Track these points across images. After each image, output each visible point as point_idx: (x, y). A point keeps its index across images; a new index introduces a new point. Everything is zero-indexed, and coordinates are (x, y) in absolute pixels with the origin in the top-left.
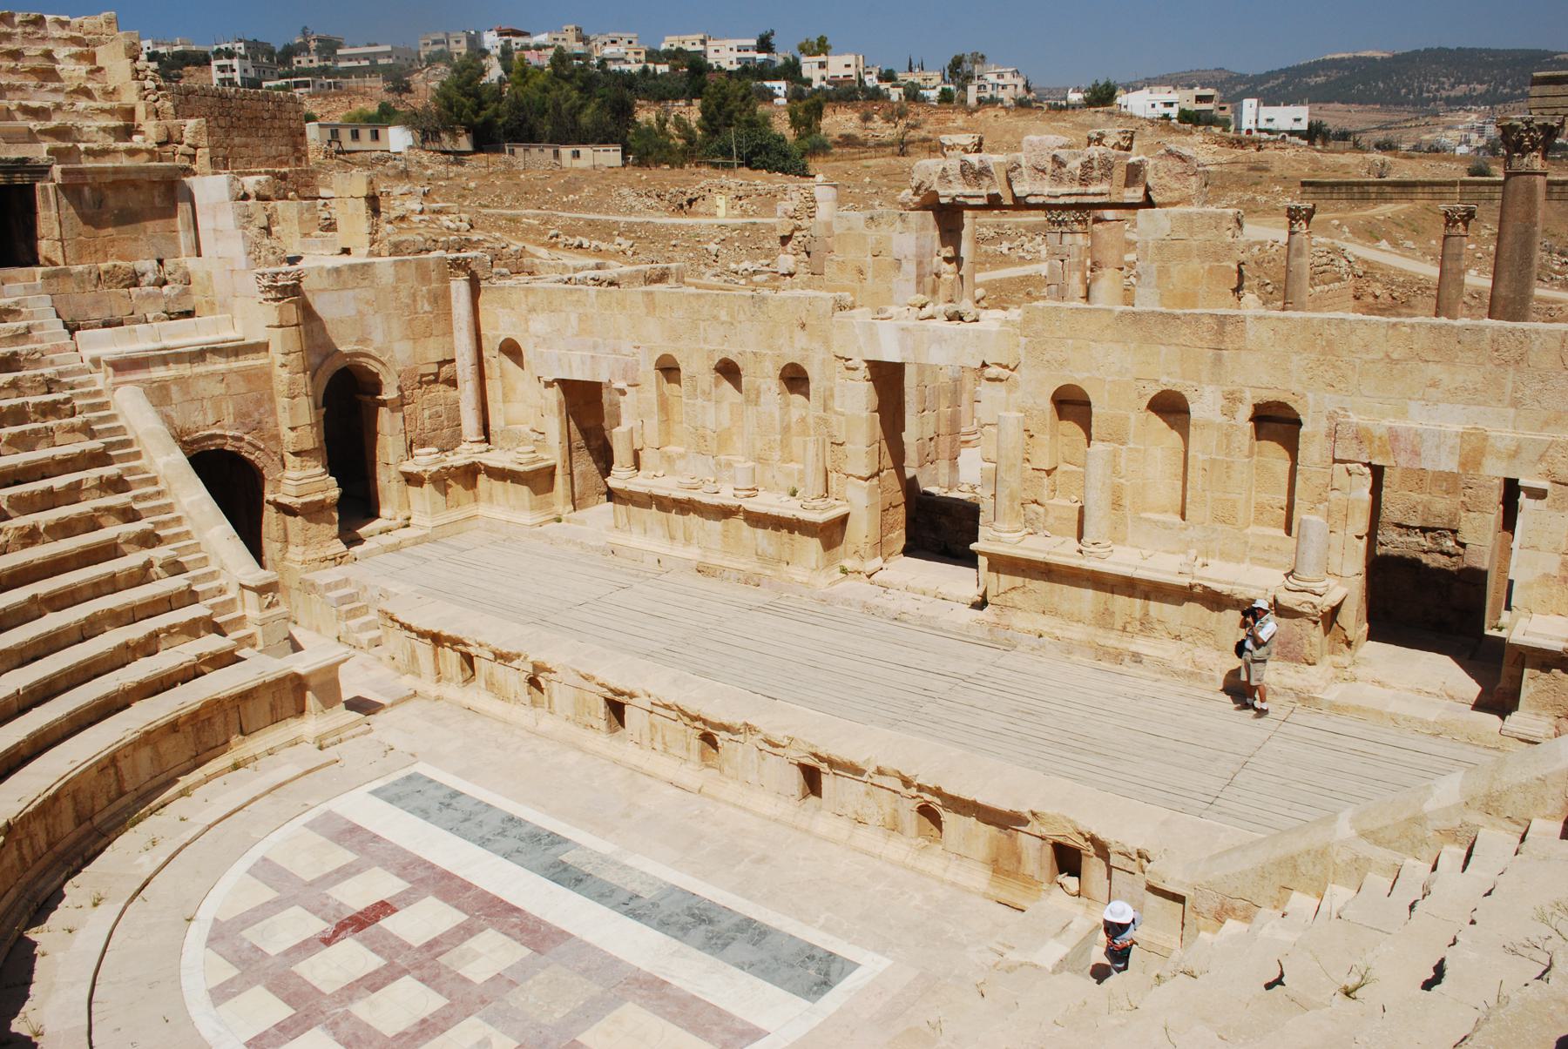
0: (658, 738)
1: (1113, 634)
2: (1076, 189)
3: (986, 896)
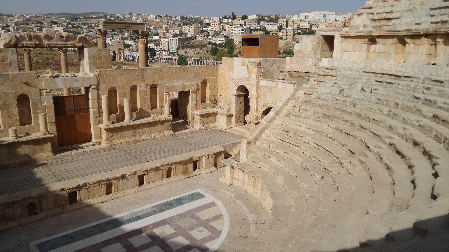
0: (92, 194)
1: (137, 137)
2: (64, 43)
3: (185, 178)
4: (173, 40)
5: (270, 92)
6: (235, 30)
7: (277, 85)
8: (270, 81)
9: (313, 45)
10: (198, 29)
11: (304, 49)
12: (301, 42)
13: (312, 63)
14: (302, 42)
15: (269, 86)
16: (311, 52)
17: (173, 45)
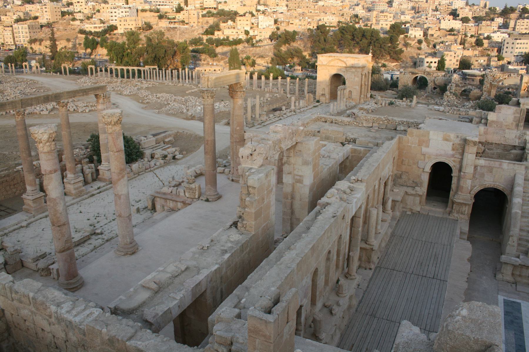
4: (20, 28)
5: (491, 172)
6: (115, 12)
7: (500, 165)
8: (491, 161)
9: (515, 117)
10: (55, 10)
11: (502, 120)
12: (498, 112)
13: (516, 136)
14: (500, 112)
15: (490, 167)
16: (512, 124)
17: (21, 37)
